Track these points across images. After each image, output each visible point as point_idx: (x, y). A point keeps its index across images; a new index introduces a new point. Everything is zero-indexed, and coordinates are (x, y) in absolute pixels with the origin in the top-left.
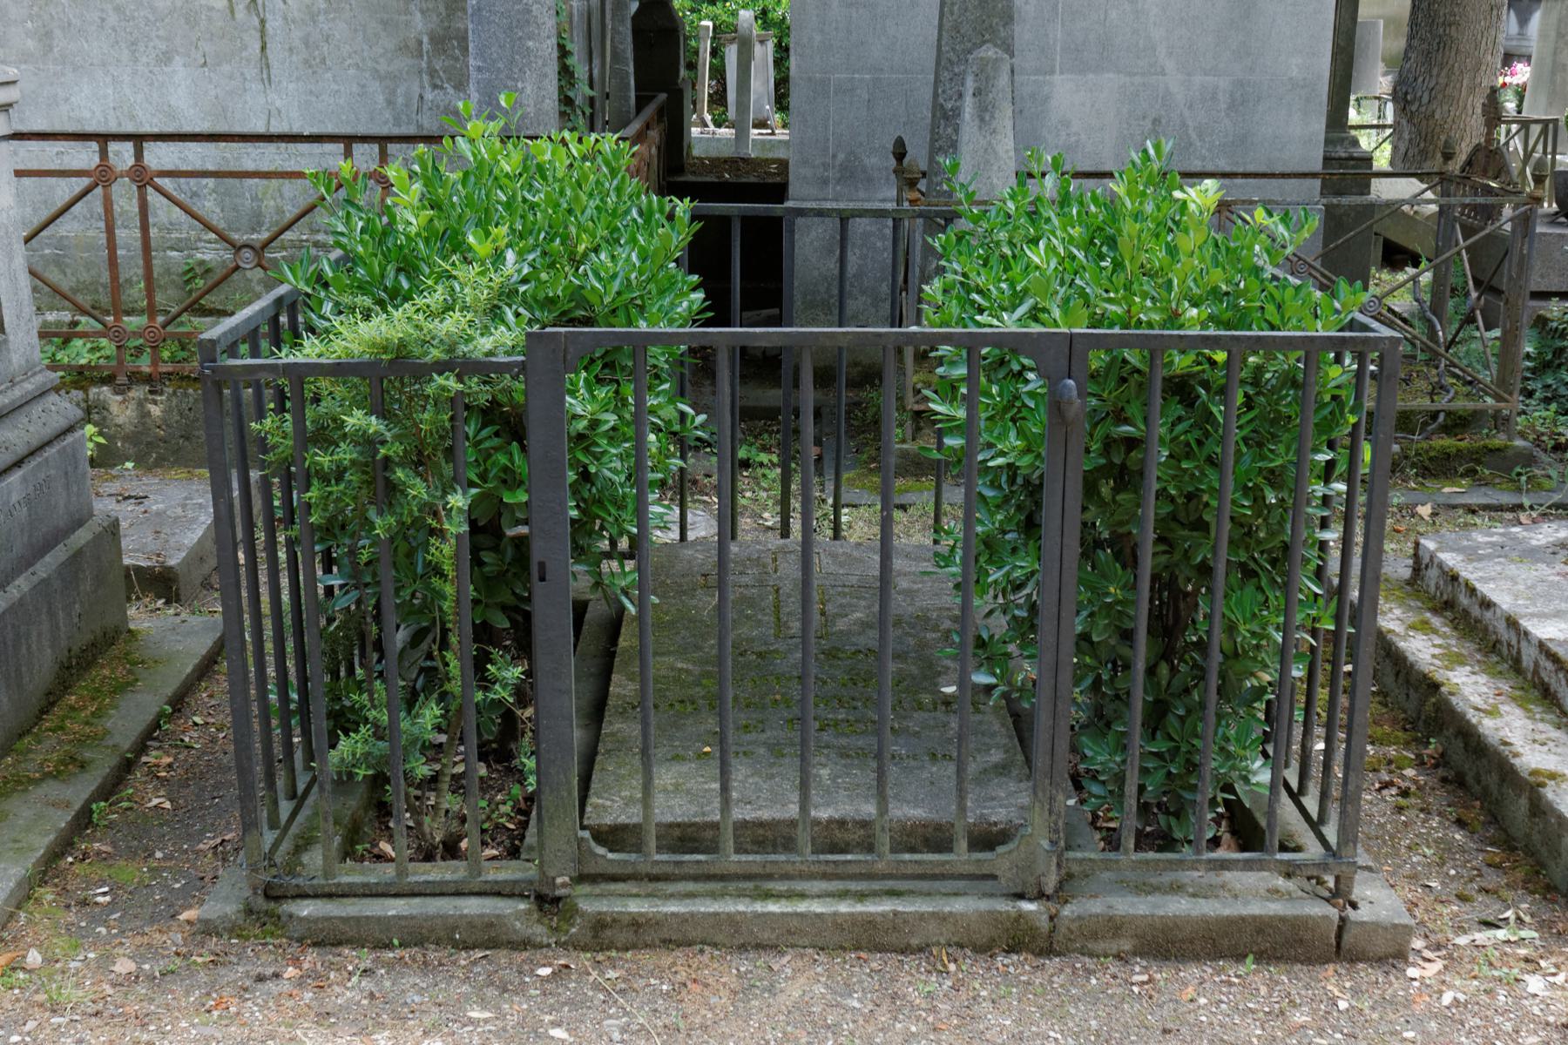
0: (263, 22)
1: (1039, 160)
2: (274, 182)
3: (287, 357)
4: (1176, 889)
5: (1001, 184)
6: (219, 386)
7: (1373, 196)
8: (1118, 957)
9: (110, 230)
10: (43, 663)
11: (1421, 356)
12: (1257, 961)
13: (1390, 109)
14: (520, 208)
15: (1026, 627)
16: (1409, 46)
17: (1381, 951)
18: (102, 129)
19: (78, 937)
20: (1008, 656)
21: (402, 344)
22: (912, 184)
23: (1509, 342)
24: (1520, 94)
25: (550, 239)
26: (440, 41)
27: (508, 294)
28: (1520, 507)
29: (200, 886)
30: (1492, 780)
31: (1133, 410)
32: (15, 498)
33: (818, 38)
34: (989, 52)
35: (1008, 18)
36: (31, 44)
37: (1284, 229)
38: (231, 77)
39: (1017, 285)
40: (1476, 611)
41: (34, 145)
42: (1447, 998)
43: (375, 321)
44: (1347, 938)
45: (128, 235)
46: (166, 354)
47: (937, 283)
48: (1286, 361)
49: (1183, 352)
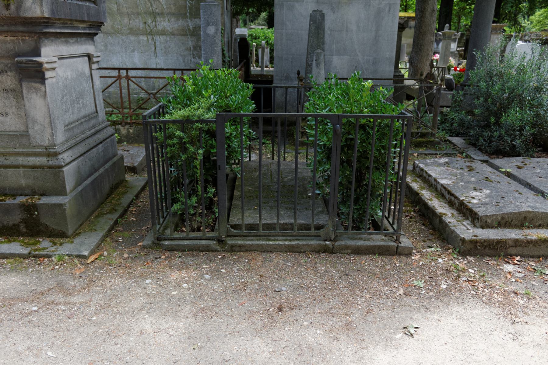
0: (155, 43)
1: (331, 75)
2: (158, 79)
3: (162, 119)
4: (361, 239)
5: (322, 81)
6: (147, 125)
7: (404, 84)
8: (348, 254)
9: (121, 90)
10: (107, 187)
11: (415, 120)
12: (379, 255)
13: (408, 64)
14: (215, 86)
15: (327, 180)
16: (413, 50)
17: (406, 253)
18: (119, 67)
19: (115, 249)
20: (323, 187)
21: (188, 116)
22: (301, 81)
23: (435, 117)
24: (437, 61)
25: (221, 93)
26: (195, 48)
27: (212, 105)
28: (437, 154)
29: (142, 238)
30: (431, 215)
31: (352, 132)
32: (100, 150)
33: (280, 47)
34: (319, 51)
35: (323, 43)
36: (102, 48)
37: (385, 91)
38: (148, 55)
39: (326, 103)
40: (427, 177)
41: (103, 71)
42: (421, 263)
43: (182, 111)
44: (399, 250)
45: (125, 91)
46: (133, 118)
47: (308, 103)
48: (388, 121)
49: (363, 119)
